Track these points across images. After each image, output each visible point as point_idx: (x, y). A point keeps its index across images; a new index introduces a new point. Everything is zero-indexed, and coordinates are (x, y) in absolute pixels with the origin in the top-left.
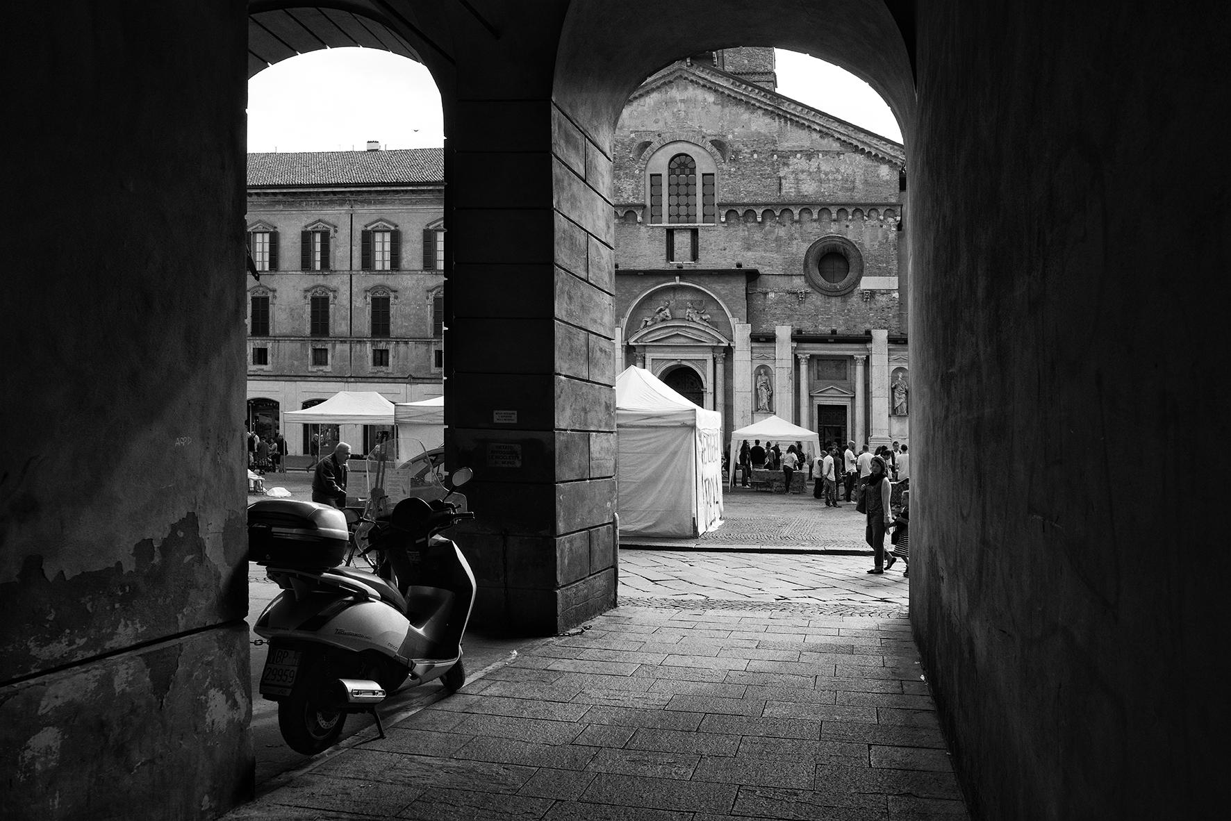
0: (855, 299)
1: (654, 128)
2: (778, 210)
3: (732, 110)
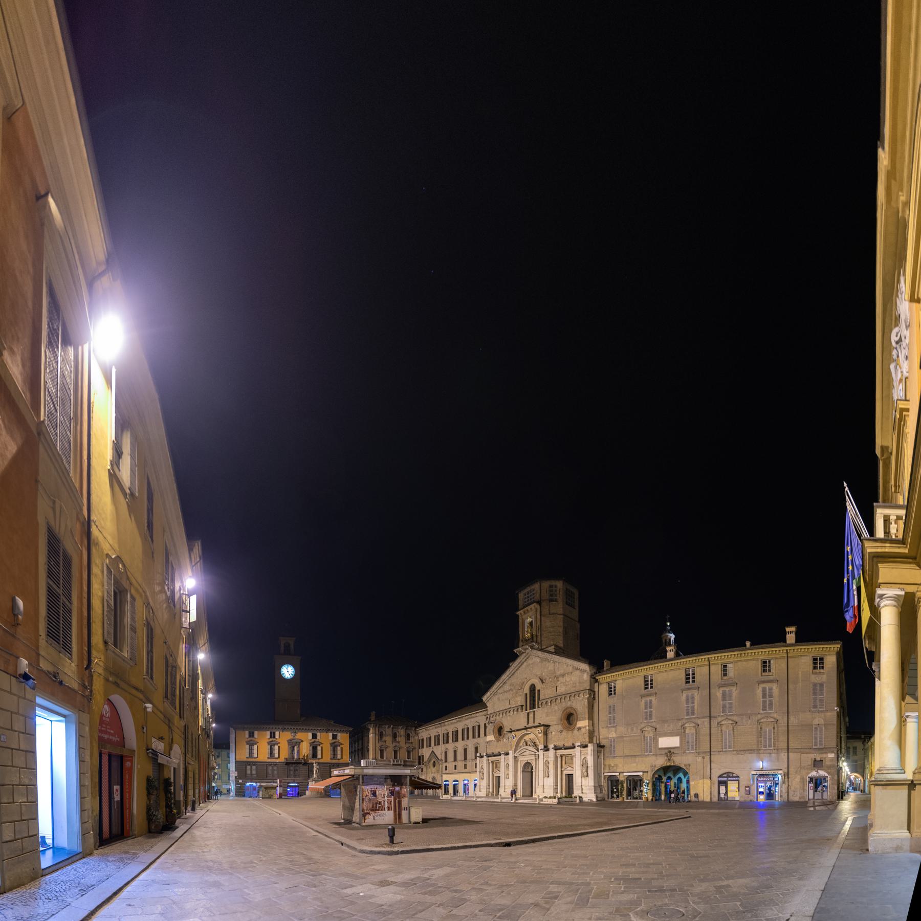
0: (576, 732)
2: (553, 700)
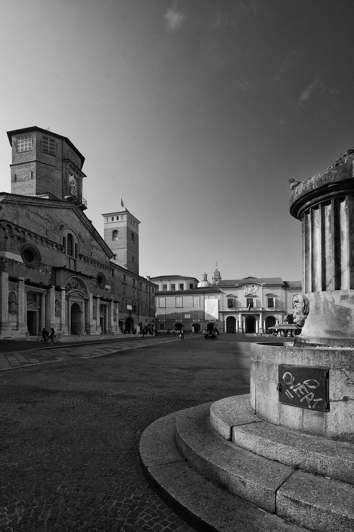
1: (66, 222)
3: (83, 228)
